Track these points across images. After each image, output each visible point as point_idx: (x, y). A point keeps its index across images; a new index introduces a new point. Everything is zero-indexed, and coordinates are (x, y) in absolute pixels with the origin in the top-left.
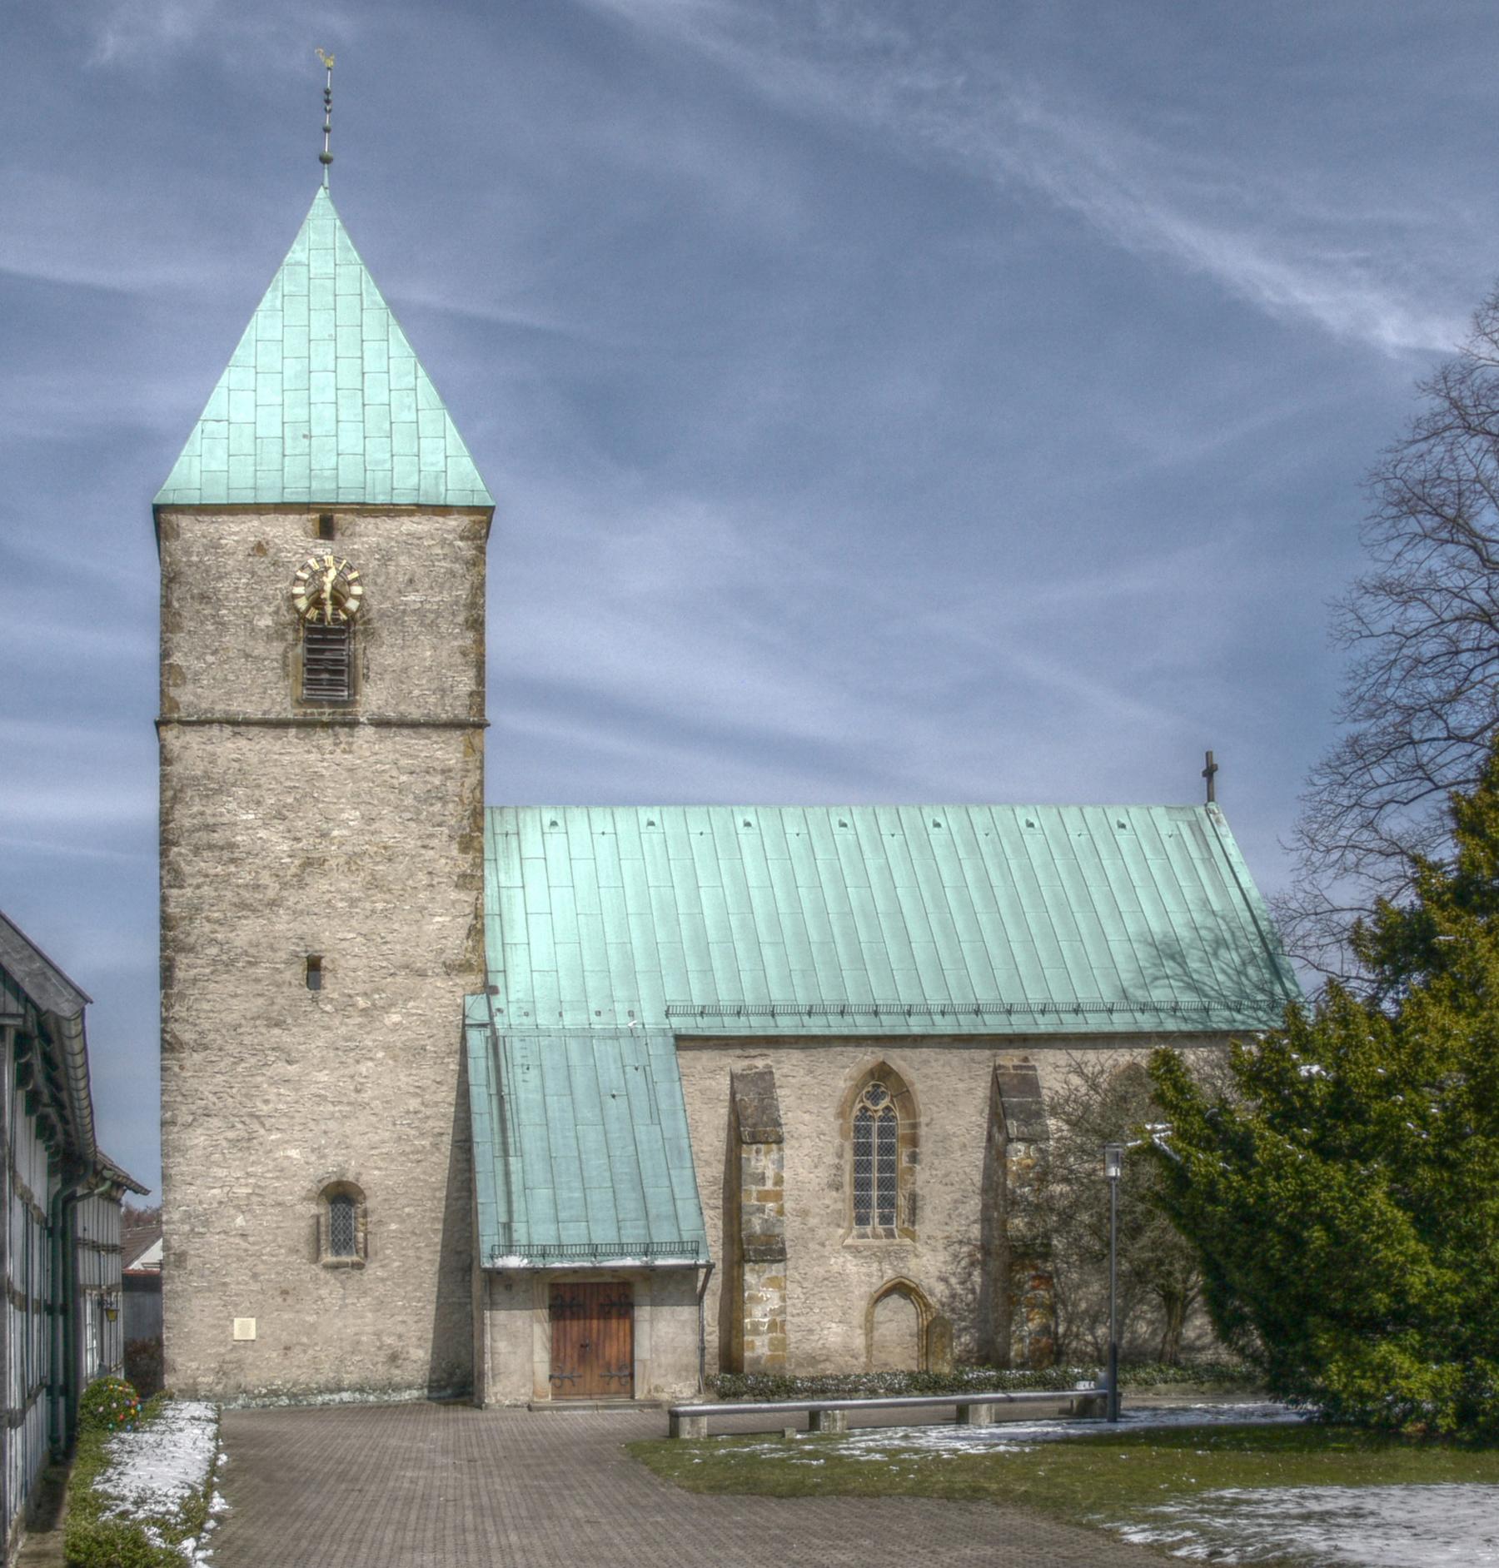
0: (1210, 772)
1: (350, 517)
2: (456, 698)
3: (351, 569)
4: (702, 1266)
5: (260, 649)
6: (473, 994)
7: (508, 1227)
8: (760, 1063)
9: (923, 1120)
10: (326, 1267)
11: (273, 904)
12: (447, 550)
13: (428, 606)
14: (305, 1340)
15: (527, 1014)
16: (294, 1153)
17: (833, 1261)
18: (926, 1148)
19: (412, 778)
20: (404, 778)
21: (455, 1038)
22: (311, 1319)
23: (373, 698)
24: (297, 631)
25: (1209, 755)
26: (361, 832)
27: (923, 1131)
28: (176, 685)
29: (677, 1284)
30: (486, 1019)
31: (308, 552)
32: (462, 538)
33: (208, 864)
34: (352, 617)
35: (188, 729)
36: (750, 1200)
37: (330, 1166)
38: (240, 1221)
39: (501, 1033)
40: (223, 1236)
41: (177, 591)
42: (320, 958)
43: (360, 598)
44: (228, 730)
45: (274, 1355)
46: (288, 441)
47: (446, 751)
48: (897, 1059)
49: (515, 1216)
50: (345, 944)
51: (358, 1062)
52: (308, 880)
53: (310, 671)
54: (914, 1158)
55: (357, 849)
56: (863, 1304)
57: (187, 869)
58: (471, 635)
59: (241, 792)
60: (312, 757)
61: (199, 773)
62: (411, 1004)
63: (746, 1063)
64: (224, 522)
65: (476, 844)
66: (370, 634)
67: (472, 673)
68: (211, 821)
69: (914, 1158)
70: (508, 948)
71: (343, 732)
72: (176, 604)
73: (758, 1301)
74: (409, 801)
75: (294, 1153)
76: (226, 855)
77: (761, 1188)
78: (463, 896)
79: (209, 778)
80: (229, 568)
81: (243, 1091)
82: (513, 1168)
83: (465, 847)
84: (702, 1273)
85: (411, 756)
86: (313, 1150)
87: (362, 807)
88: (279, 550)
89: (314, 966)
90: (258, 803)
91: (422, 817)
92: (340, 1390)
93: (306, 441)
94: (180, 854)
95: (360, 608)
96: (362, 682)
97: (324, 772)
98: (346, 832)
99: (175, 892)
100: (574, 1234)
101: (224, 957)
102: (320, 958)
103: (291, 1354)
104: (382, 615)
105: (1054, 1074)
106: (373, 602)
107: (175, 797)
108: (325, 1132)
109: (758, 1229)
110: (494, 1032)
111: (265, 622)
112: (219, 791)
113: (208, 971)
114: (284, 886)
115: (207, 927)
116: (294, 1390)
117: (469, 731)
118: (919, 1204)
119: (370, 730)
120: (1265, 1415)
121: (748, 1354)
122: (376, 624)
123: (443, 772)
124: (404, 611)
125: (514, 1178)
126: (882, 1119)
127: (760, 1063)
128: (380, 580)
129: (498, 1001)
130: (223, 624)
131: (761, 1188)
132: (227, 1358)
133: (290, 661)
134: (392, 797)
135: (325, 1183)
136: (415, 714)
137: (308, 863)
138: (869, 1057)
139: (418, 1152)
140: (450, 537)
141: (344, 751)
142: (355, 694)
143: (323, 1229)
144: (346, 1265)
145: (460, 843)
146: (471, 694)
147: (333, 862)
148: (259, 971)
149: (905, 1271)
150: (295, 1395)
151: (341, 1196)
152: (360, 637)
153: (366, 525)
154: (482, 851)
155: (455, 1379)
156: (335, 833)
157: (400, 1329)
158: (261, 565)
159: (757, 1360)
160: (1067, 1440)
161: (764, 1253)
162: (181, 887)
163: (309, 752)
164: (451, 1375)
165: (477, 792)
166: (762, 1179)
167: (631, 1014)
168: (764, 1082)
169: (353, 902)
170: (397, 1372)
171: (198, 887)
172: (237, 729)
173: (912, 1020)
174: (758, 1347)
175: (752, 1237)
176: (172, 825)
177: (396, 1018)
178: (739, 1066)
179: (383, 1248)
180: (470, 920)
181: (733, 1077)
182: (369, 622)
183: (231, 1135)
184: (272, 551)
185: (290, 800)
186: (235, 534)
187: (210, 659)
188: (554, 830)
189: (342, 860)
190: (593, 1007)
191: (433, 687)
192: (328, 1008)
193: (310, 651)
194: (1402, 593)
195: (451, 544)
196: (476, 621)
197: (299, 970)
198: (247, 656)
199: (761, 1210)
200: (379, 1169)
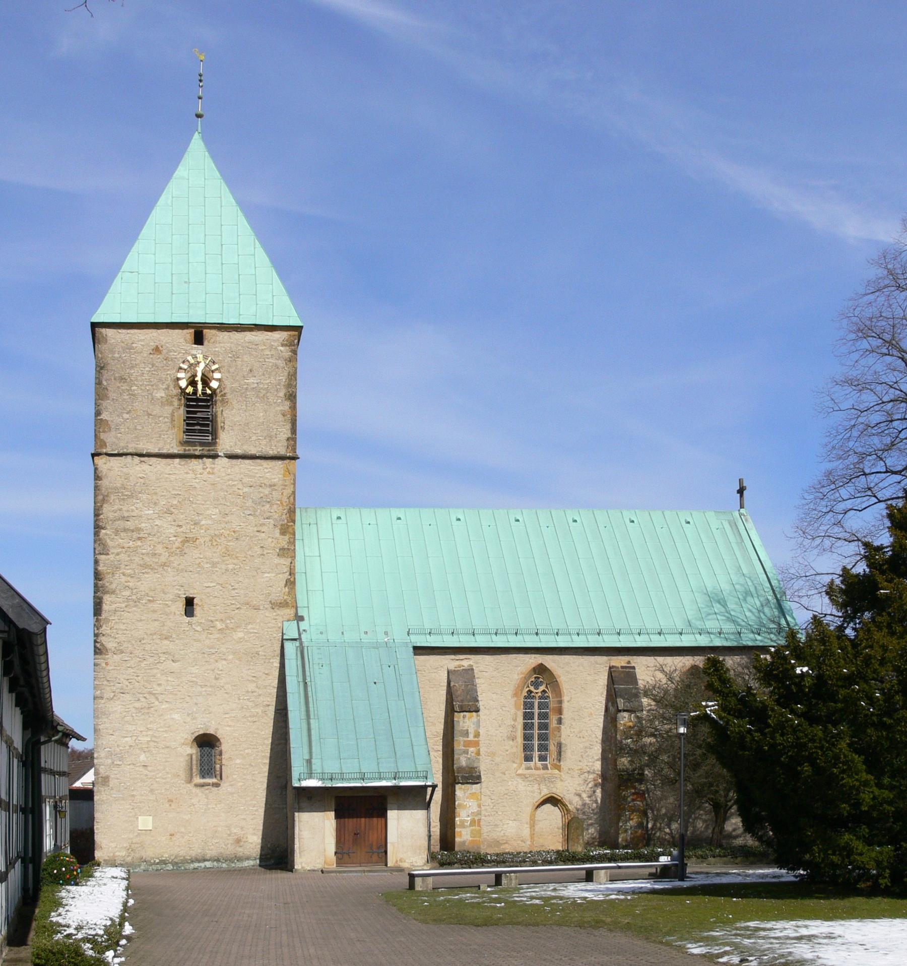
0: (741, 491)
1: (214, 332)
2: (278, 442)
3: (214, 363)
4: (429, 786)
5: (157, 410)
6: (288, 621)
7: (309, 762)
10: (196, 785)
11: (164, 565)
12: (273, 352)
13: (261, 386)
14: (183, 830)
15: (321, 633)
16: (176, 716)
17: (510, 783)
18: (566, 716)
19: (251, 490)
22: (187, 817)
23: (226, 441)
24: (180, 400)
28: (104, 432)
29: (413, 797)
30: (296, 636)
32: (283, 345)
33: (123, 540)
34: (214, 391)
35: (112, 458)
36: (459, 746)
38: (143, 757)
39: (305, 644)
40: (132, 766)
41: (106, 375)
42: (193, 598)
43: (219, 380)
44: (137, 459)
45: (164, 839)
47: (273, 472)
48: (549, 661)
49: (314, 755)
50: (208, 590)
52: (186, 551)
53: (188, 425)
54: (560, 721)
55: (217, 532)
56: (529, 809)
57: (110, 543)
58: (288, 403)
59: (144, 497)
61: (119, 485)
62: (250, 626)
63: (458, 663)
64: (135, 334)
65: (290, 530)
66: (224, 402)
67: (289, 426)
68: (126, 514)
70: (310, 593)
71: (208, 461)
72: (105, 383)
73: (465, 807)
74: (249, 503)
75: (176, 716)
76: (135, 535)
77: (466, 739)
79: (125, 488)
80: (138, 362)
81: (145, 679)
82: (312, 726)
83: (283, 532)
84: (429, 790)
85: (251, 477)
87: (220, 507)
88: (170, 351)
89: (190, 603)
90: (155, 504)
91: (257, 513)
92: (205, 860)
93: (186, 285)
94: (106, 534)
96: (220, 432)
97: (196, 485)
98: (210, 522)
99: (102, 557)
100: (350, 767)
101: (134, 597)
102: (193, 598)
103: (174, 838)
104: (233, 390)
105: (647, 672)
106: (226, 382)
107: (103, 500)
108: (196, 704)
110: (301, 643)
111: (160, 394)
113: (123, 605)
114: (171, 554)
115: (123, 579)
116: (176, 860)
117: (287, 461)
118: (563, 749)
120: (774, 877)
121: (457, 839)
122: (229, 396)
123: (270, 486)
124: (247, 389)
125: (313, 732)
126: (540, 698)
128: (232, 370)
129: (303, 625)
130: (134, 395)
131: (466, 739)
132: (134, 841)
133: (176, 418)
135: (197, 734)
136: (253, 451)
137: (186, 540)
139: (254, 716)
140: (276, 344)
141: (209, 473)
143: (194, 762)
144: (208, 785)
145: (281, 529)
146: (288, 439)
147: (202, 540)
148: (155, 606)
149: (554, 790)
150: (177, 863)
151: (207, 743)
152: (219, 404)
153: (224, 336)
154: (294, 534)
156: (203, 522)
158: (158, 359)
159: (464, 842)
160: (654, 892)
161: (467, 778)
162: (108, 554)
163: (187, 473)
166: (467, 733)
167: (386, 633)
169: (214, 565)
170: (240, 849)
171: (118, 554)
172: (142, 459)
173: (559, 638)
174: (463, 836)
175: (461, 769)
176: (101, 516)
177: (241, 635)
180: (287, 576)
182: (224, 395)
183: (138, 705)
184: (165, 352)
185: (175, 502)
186: (142, 340)
187: (126, 416)
188: (339, 521)
189: (207, 539)
190: (363, 629)
191: (265, 434)
192: (199, 628)
193: (188, 412)
194: (859, 385)
195: (276, 348)
196: (291, 395)
197: (181, 606)
199: (466, 752)
200: (230, 726)
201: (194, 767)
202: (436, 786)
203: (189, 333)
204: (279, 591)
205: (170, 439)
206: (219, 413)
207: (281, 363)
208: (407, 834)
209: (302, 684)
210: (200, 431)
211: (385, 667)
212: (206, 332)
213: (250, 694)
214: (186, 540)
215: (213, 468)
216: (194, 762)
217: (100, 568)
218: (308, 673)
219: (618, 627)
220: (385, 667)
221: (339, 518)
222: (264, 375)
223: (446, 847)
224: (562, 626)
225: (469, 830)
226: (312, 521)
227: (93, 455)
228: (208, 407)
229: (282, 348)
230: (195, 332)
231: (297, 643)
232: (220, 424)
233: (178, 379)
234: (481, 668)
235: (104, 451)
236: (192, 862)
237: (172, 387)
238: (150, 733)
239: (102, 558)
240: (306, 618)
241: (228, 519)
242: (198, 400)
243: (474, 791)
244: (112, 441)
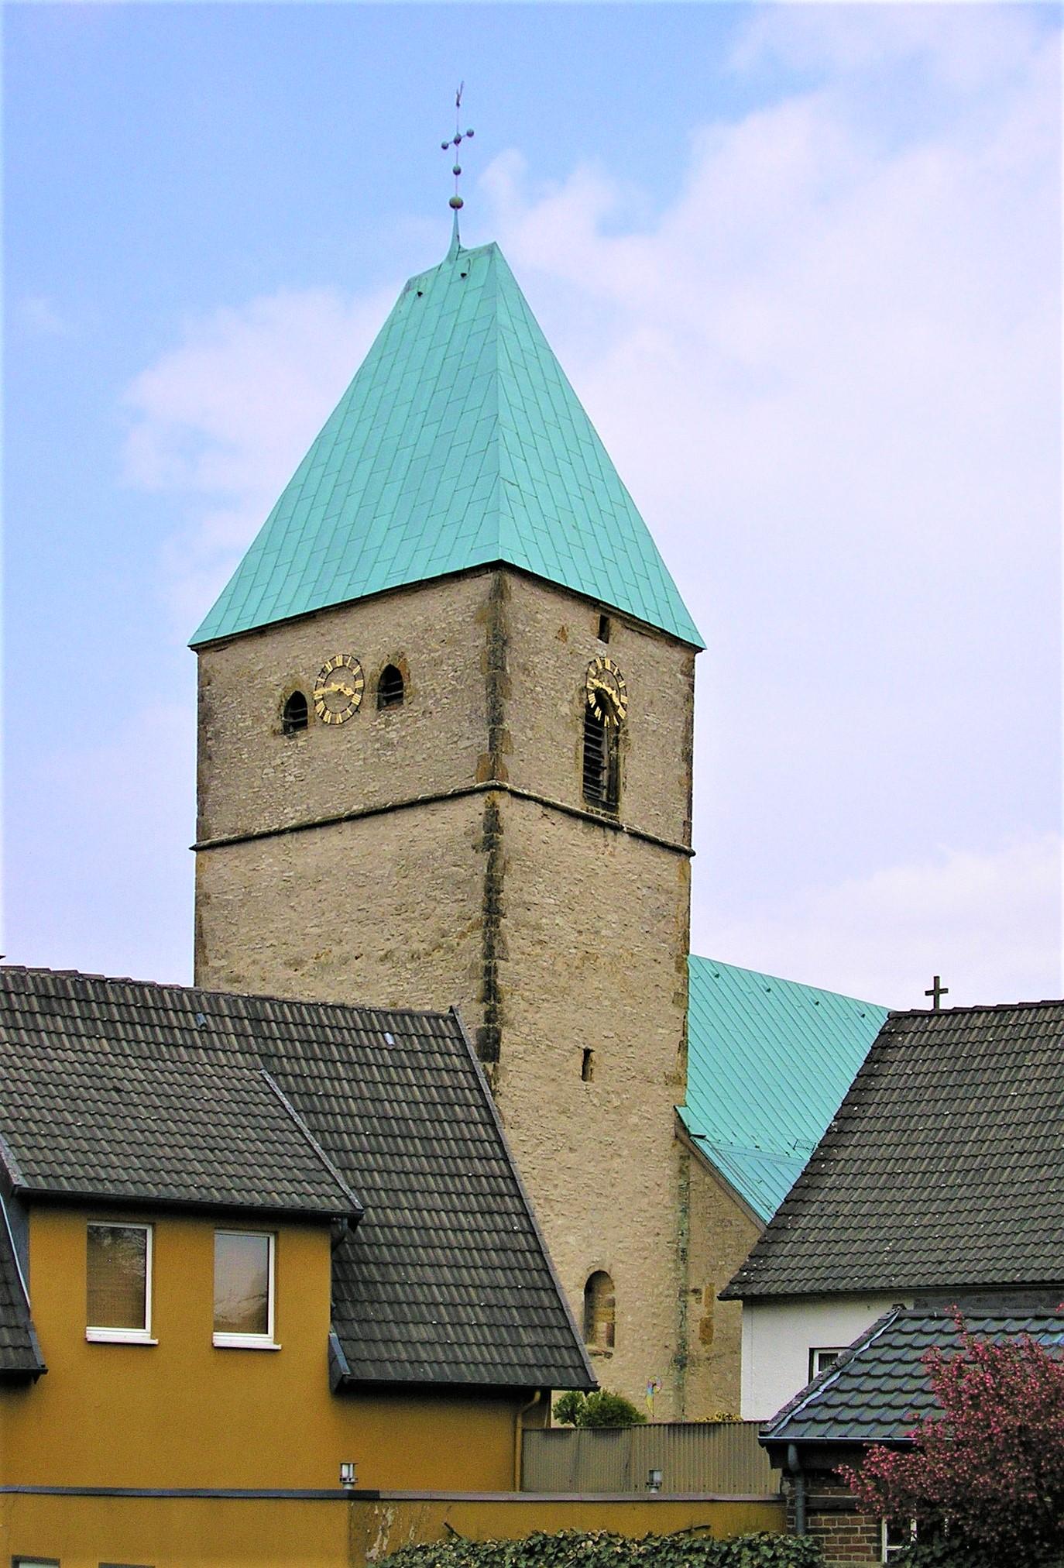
11: (565, 991)
16: (571, 1239)
25: (936, 978)
57: (509, 941)
68: (527, 898)
71: (610, 833)
75: (571, 1239)
80: (543, 646)
81: (542, 1173)
88: (575, 641)
96: (622, 789)
101: (532, 1037)
111: (565, 709)
112: (533, 870)
113: (521, 1048)
139: (643, 1249)
147: (601, 961)
179: (623, 1339)
182: (626, 733)
186: (548, 612)
187: (530, 734)
229: (680, 676)
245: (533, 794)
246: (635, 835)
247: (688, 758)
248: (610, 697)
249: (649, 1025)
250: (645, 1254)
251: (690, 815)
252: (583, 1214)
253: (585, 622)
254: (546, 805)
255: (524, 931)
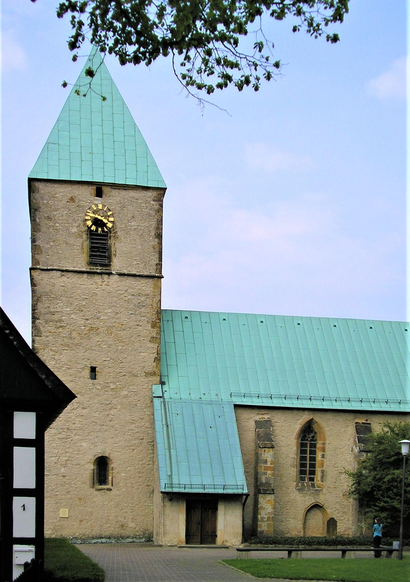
4: (245, 495)
5: (71, 240)
6: (156, 384)
7: (171, 476)
8: (266, 417)
9: (327, 442)
10: (96, 490)
13: (140, 228)
14: (87, 518)
15: (176, 393)
17: (291, 495)
18: (328, 453)
19: (133, 297)
20: (129, 297)
21: (148, 401)
22: (90, 510)
23: (117, 265)
26: (113, 318)
27: (327, 446)
30: (161, 395)
31: (91, 202)
32: (154, 200)
33: (51, 327)
34: (110, 229)
35: (43, 272)
36: (261, 470)
37: (99, 451)
38: (63, 470)
39: (167, 400)
40: (56, 476)
41: (38, 215)
43: (113, 222)
45: (75, 523)
46: (83, 154)
47: (146, 286)
48: (318, 418)
51: (110, 409)
52: (91, 336)
53: (92, 251)
56: (302, 512)
57: (42, 329)
58: (157, 240)
60: (93, 286)
61: (48, 290)
62: (131, 387)
63: (261, 416)
65: (158, 325)
66: (116, 238)
67: (157, 256)
68: (52, 310)
69: (323, 456)
72: (38, 220)
74: (131, 306)
75: (84, 444)
76: (59, 324)
77: (265, 465)
78: (152, 345)
83: (153, 327)
84: (244, 497)
86: (92, 443)
87: (113, 308)
89: (93, 370)
90: (71, 304)
92: (102, 538)
93: (91, 155)
94: (40, 323)
95: (113, 227)
96: (113, 257)
99: (37, 338)
100: (196, 481)
101: (58, 365)
103: (82, 523)
105: (378, 427)
107: (38, 300)
109: (264, 481)
110: (164, 399)
111: (74, 230)
112: (56, 298)
115: (51, 353)
117: (156, 279)
119: (117, 277)
121: (259, 529)
123: (145, 295)
125: (172, 457)
126: (311, 440)
127: (266, 417)
129: (165, 387)
130: (57, 230)
131: (265, 465)
132: (57, 524)
133: (84, 247)
134: (125, 304)
135: (97, 456)
136: (134, 272)
137: (92, 329)
138: (305, 417)
140: (149, 199)
142: (110, 262)
143: (95, 475)
144: (104, 489)
145: (152, 324)
146: (157, 265)
148: (71, 371)
149: (318, 500)
152: (112, 238)
153: (115, 192)
155: (146, 535)
156: (102, 318)
157: (125, 515)
158: (72, 206)
161: (267, 490)
162: (41, 336)
163: (92, 284)
164: (144, 534)
165: (159, 304)
166: (266, 462)
167: (217, 395)
168: (268, 424)
169: (109, 346)
172: (63, 274)
173: (324, 403)
176: (36, 311)
178: (258, 418)
179: (119, 483)
181: (256, 422)
182: (116, 233)
183: (60, 436)
184: (77, 201)
186: (61, 192)
187: (52, 244)
188: (186, 320)
190: (202, 392)
192: (99, 387)
193: (92, 243)
195: (149, 202)
196: (159, 235)
197: (87, 372)
198: (67, 244)
199: (265, 474)
200: (119, 452)
201: (95, 478)
202: (249, 495)
203: (92, 190)
204: (150, 365)
205: (81, 262)
206: (113, 244)
207: (153, 213)
208: (228, 524)
209: (165, 426)
210: (100, 256)
211: (217, 417)
212: (104, 188)
213: (131, 431)
214: (92, 329)
215: (109, 282)
216: (95, 475)
217: (35, 346)
218: (168, 420)
219: (361, 397)
220: (217, 417)
221: (186, 318)
222: (141, 220)
223: (250, 534)
224: (326, 395)
225: (266, 523)
226: (170, 319)
227: (31, 269)
228: (105, 240)
229: (152, 202)
230: (97, 188)
231: (162, 400)
232: (113, 252)
233: (86, 220)
234: (276, 420)
235: (38, 267)
236: (93, 539)
237: (82, 226)
238: (68, 454)
239: (37, 338)
240: (167, 383)
241: (118, 316)
242: (100, 235)
243: (270, 499)
244: (44, 261)
245: (54, 268)
246: (121, 275)
247: (159, 236)
248: (102, 221)
249: (134, 353)
250: (133, 448)
251: (160, 259)
252: (92, 434)
253: (88, 192)
254: (62, 271)
255: (51, 323)
